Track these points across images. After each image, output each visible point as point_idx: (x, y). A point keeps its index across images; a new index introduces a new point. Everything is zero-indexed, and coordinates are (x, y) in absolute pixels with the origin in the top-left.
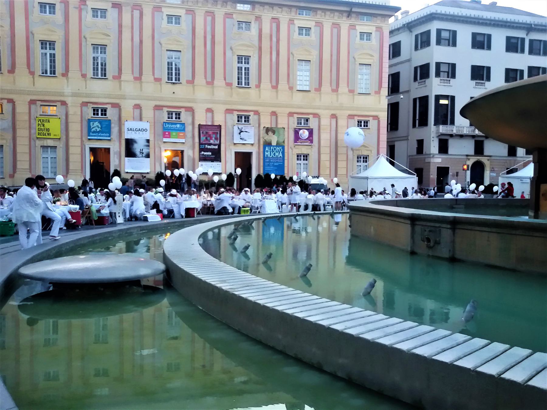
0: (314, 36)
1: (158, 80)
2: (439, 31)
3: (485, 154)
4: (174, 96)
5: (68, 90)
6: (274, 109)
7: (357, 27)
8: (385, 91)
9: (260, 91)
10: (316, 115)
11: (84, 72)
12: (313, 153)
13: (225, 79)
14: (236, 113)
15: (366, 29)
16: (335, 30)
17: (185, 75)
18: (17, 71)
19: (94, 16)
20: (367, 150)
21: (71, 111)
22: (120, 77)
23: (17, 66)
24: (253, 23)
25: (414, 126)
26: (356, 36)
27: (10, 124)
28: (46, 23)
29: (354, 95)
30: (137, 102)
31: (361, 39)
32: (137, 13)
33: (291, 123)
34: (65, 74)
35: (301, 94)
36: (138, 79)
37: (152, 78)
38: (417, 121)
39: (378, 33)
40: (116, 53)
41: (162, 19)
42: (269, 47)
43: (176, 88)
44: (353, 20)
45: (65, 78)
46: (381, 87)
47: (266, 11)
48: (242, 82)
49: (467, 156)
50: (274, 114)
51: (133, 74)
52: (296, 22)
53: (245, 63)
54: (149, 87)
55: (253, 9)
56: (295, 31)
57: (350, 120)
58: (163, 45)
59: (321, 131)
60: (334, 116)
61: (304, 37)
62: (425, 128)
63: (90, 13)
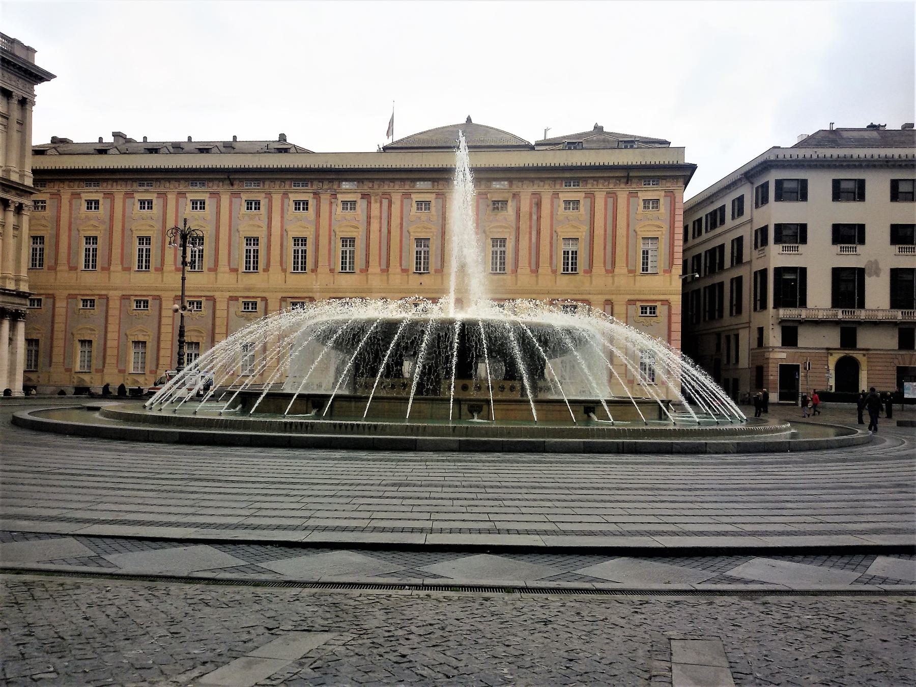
1: (405, 271)
2: (779, 183)
3: (858, 346)
5: (316, 286)
7: (640, 194)
8: (678, 270)
9: (516, 276)
11: (332, 267)
15: (650, 196)
16: (610, 200)
19: (343, 209)
23: (271, 264)
24: (510, 202)
25: (755, 309)
28: (299, 220)
29: (635, 276)
36: (386, 270)
37: (399, 270)
38: (758, 303)
39: (669, 198)
40: (364, 246)
43: (425, 279)
46: (673, 264)
47: (525, 187)
49: (828, 349)
52: (561, 195)
55: (511, 186)
57: (629, 307)
61: (570, 212)
62: (765, 312)
63: (340, 206)
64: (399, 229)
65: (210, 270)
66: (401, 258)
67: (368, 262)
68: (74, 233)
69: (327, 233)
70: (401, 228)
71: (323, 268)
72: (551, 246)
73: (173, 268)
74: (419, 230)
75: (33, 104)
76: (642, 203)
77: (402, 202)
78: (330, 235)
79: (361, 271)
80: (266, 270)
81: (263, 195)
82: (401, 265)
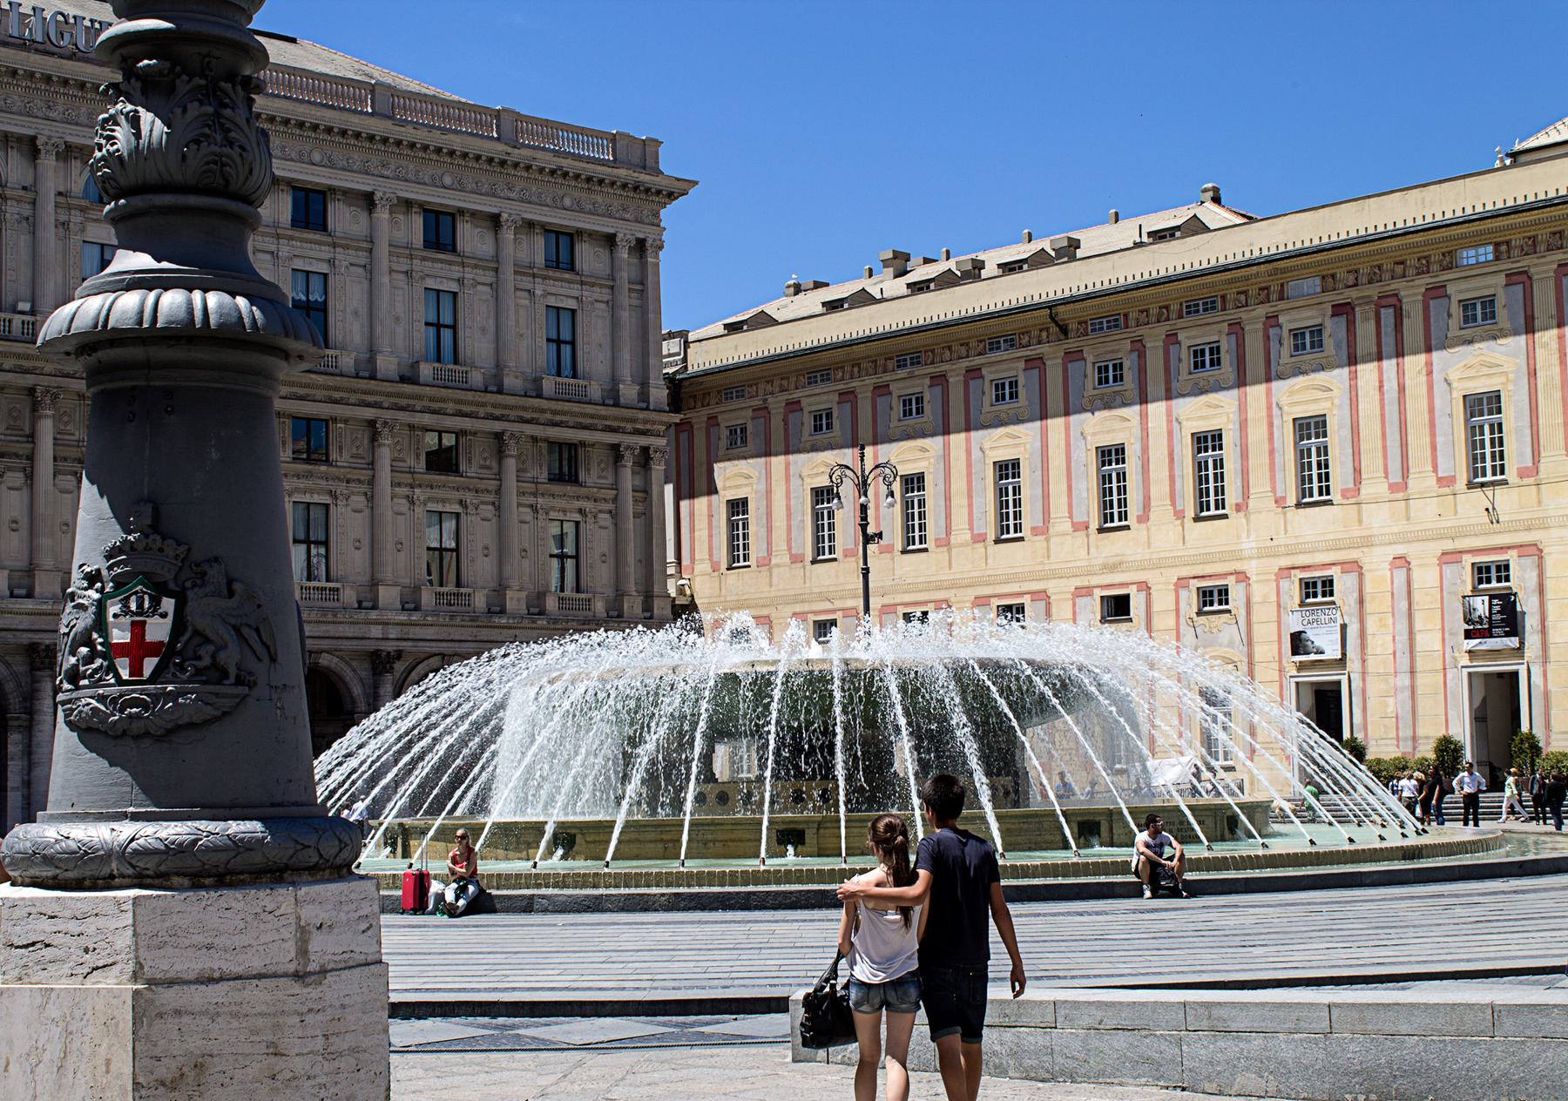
5: (1249, 544)
11: (1279, 494)
21: (1258, 592)
30: (1400, 550)
32: (1387, 315)
37: (1432, 481)
41: (1449, 315)
45: (1241, 514)
51: (1386, 477)
54: (1428, 510)
58: (1455, 385)
63: (1288, 342)
64: (1424, 378)
65: (1036, 531)
66: (1434, 448)
67: (1357, 471)
68: (795, 482)
69: (1264, 413)
70: (1430, 373)
73: (968, 536)
74: (1471, 373)
75: (661, 247)
78: (1270, 416)
80: (1144, 518)
82: (1435, 470)
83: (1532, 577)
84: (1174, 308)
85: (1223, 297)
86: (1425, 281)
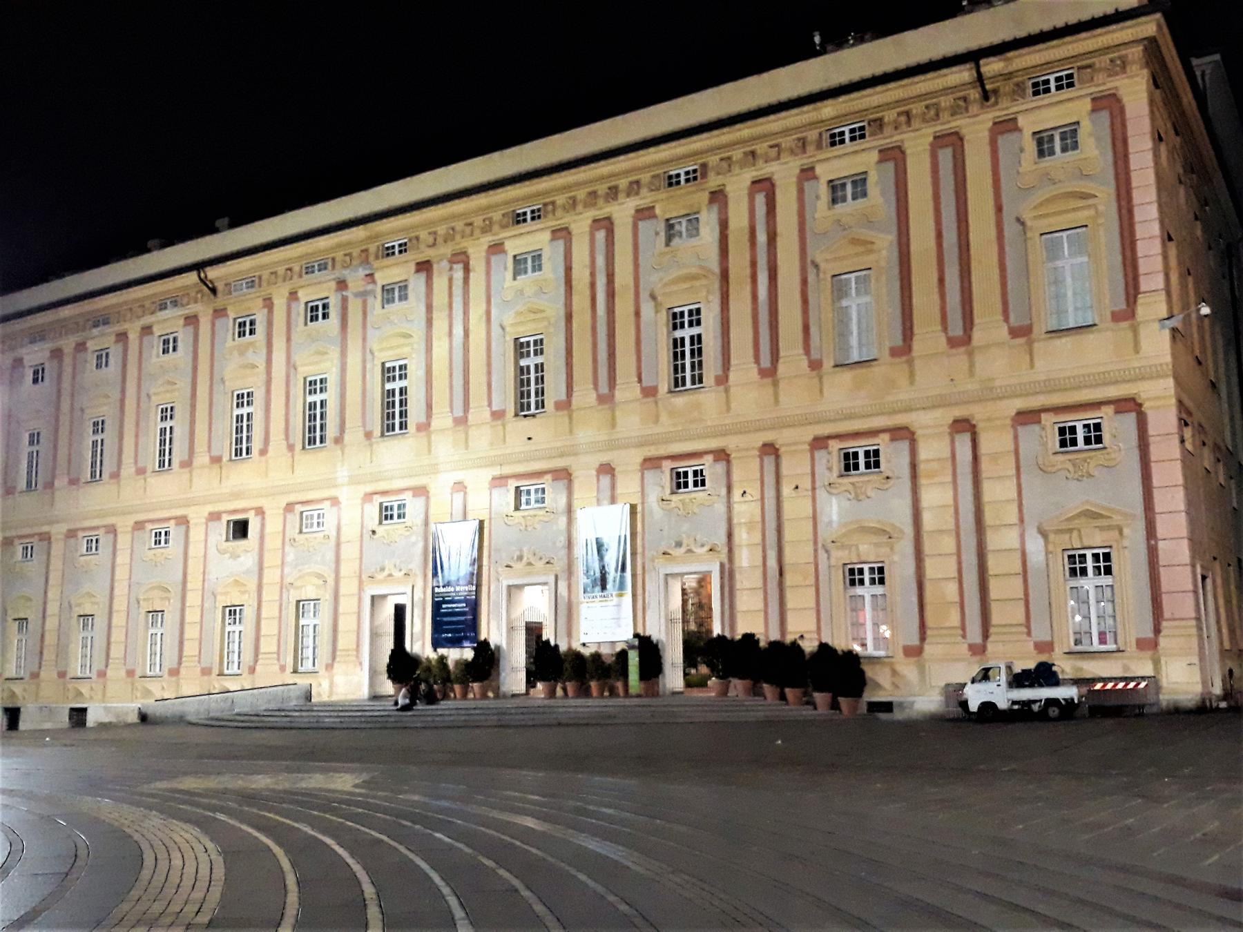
0: (879, 197)
4: (531, 446)
6: (768, 437)
7: (1021, 121)
8: (1153, 307)
9: (727, 391)
10: (902, 433)
12: (896, 558)
13: (640, 380)
14: (667, 465)
16: (946, 156)
17: (554, 388)
18: (270, 448)
20: (1101, 529)
22: (429, 425)
26: (1022, 150)
27: (256, 558)
29: (1030, 344)
31: (1041, 153)
32: (459, 274)
33: (820, 469)
34: (338, 440)
35: (847, 376)
36: (462, 421)
37: (487, 414)
40: (421, 373)
42: (747, 263)
44: (1004, 102)
45: (338, 447)
46: (1137, 291)
48: (684, 378)
50: (770, 450)
53: (691, 325)
56: (818, 197)
58: (508, 329)
59: (923, 481)
60: (964, 426)
61: (849, 207)
67: (429, 407)
71: (354, 435)
72: (805, 301)
76: (1031, 147)
77: (488, 263)
79: (419, 428)
80: (263, 452)
81: (260, 302)
82: (490, 405)
83: (562, 501)
84: (296, 269)
85: (333, 259)
86: (487, 240)
